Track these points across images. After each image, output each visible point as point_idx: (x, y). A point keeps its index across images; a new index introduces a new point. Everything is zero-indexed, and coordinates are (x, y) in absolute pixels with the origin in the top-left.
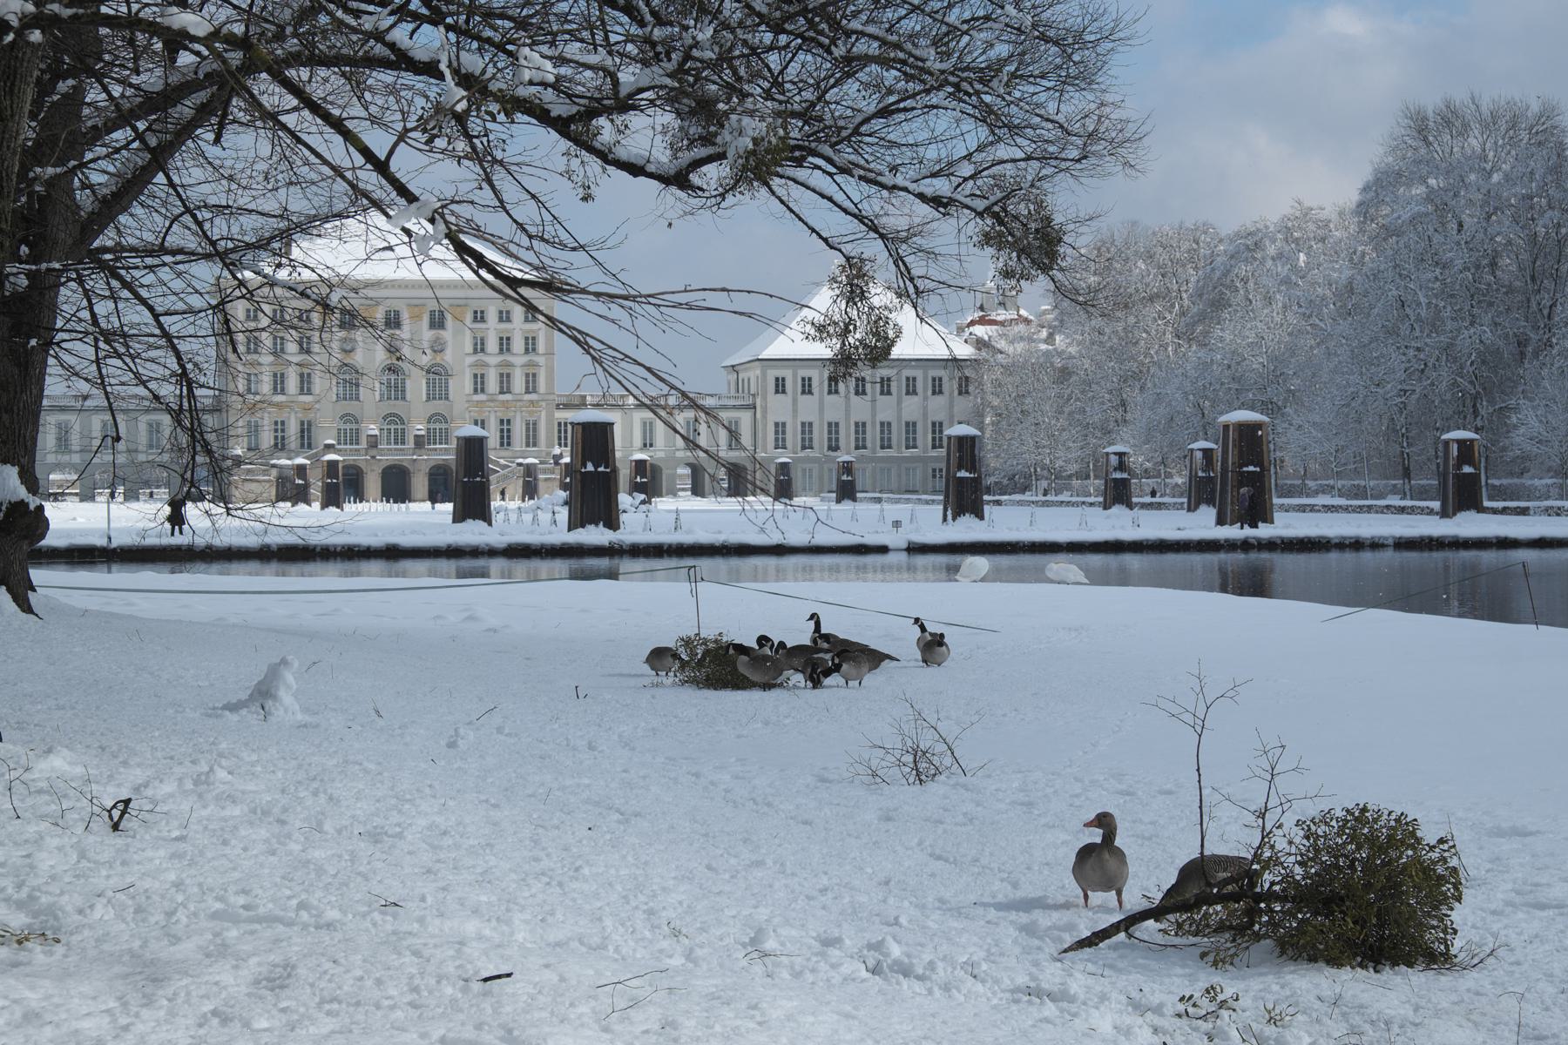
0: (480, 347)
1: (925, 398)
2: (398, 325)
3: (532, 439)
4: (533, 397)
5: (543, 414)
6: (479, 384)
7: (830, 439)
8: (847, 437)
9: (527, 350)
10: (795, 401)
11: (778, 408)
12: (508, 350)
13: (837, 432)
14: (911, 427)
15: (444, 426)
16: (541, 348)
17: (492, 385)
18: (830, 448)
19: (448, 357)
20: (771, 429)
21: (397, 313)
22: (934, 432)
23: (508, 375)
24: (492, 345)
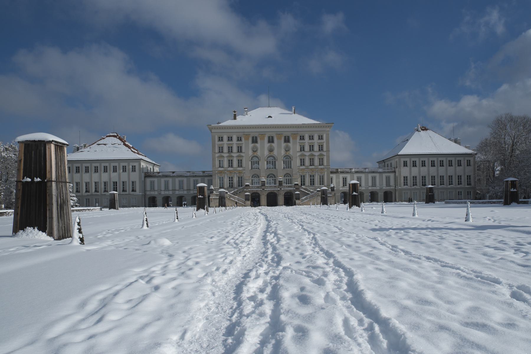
0: (302, 149)
1: (455, 167)
2: (273, 142)
3: (322, 182)
4: (322, 167)
5: (326, 173)
6: (302, 162)
7: (422, 182)
8: (428, 180)
9: (319, 150)
10: (410, 169)
11: (405, 172)
12: (313, 150)
13: (425, 180)
14: (451, 177)
15: (290, 178)
16: (325, 149)
17: (307, 162)
18: (423, 185)
19: (291, 153)
20: (402, 179)
21: (272, 137)
22: (458, 179)
23: (313, 159)
24: (307, 148)
